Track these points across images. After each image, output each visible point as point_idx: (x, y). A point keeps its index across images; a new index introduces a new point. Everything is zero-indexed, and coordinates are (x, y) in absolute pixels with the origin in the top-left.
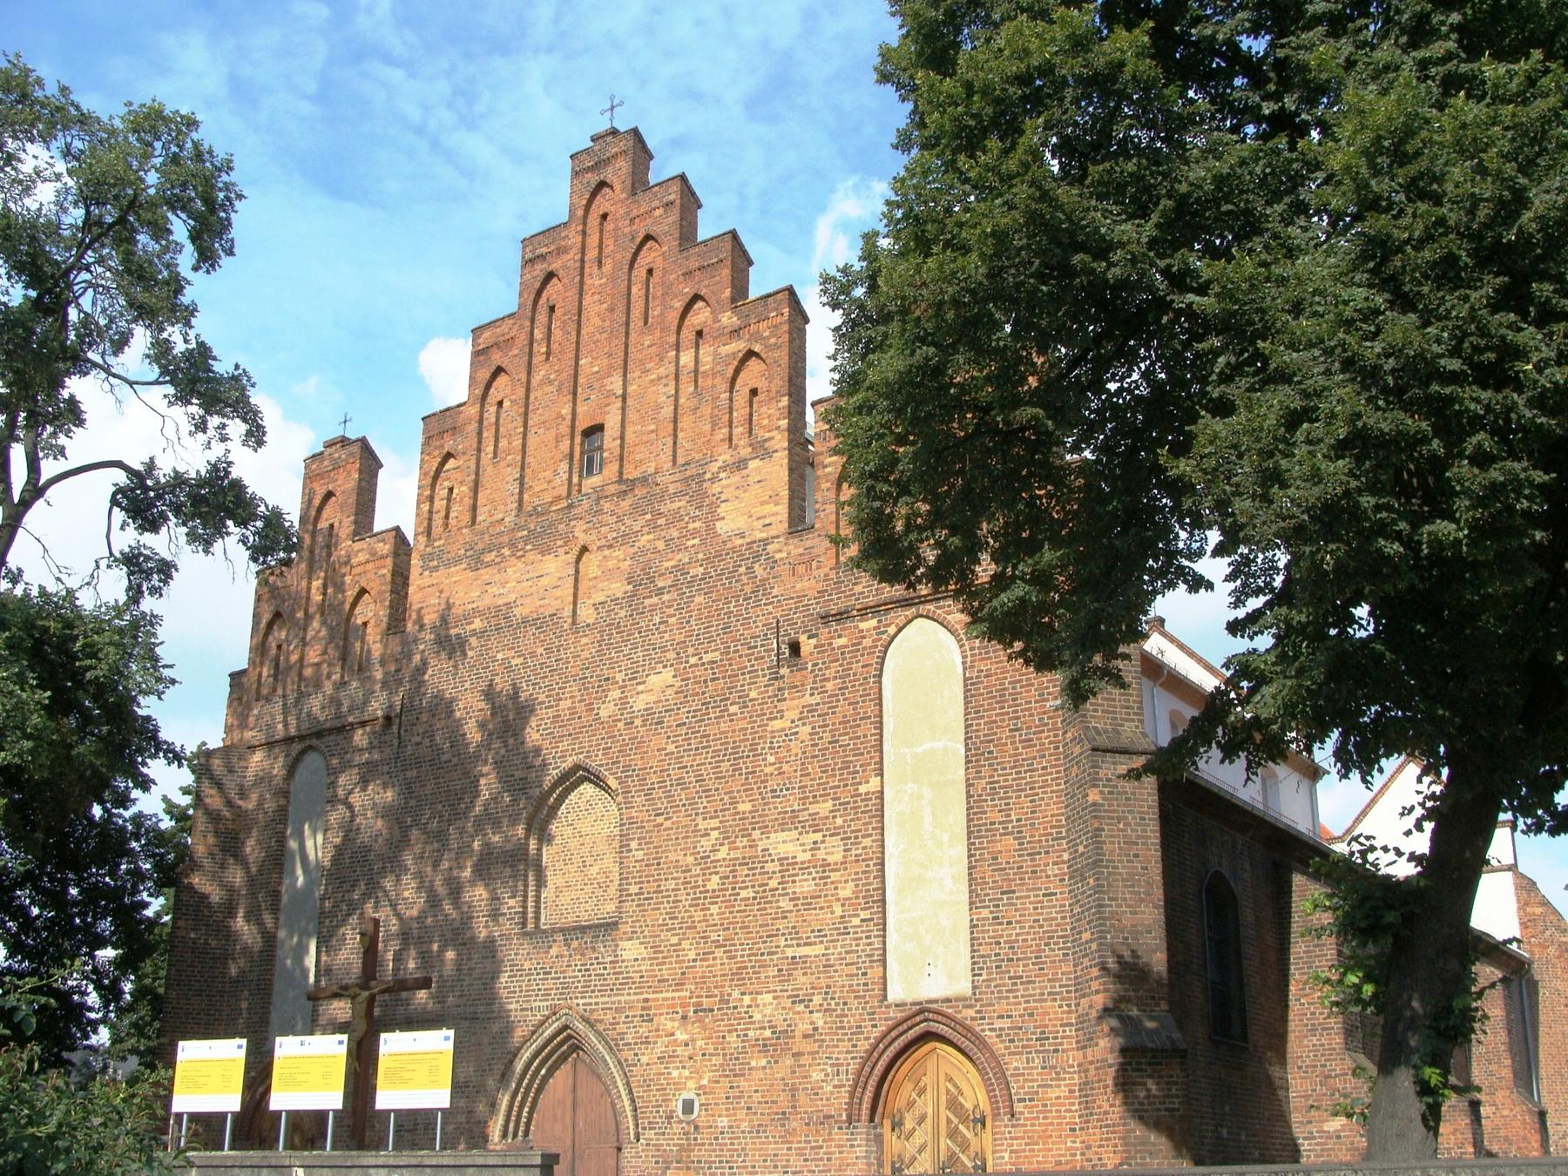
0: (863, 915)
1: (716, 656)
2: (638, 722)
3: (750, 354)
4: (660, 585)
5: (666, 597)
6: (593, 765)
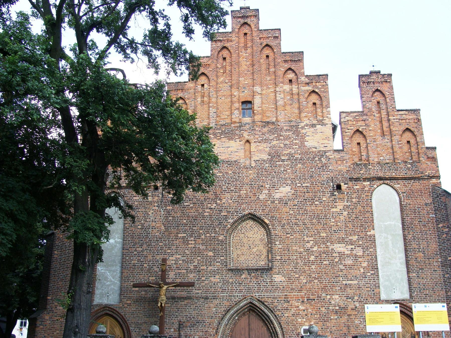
0: (372, 272)
2: (277, 202)
3: (314, 92)
4: (283, 158)
5: (286, 163)
6: (258, 214)
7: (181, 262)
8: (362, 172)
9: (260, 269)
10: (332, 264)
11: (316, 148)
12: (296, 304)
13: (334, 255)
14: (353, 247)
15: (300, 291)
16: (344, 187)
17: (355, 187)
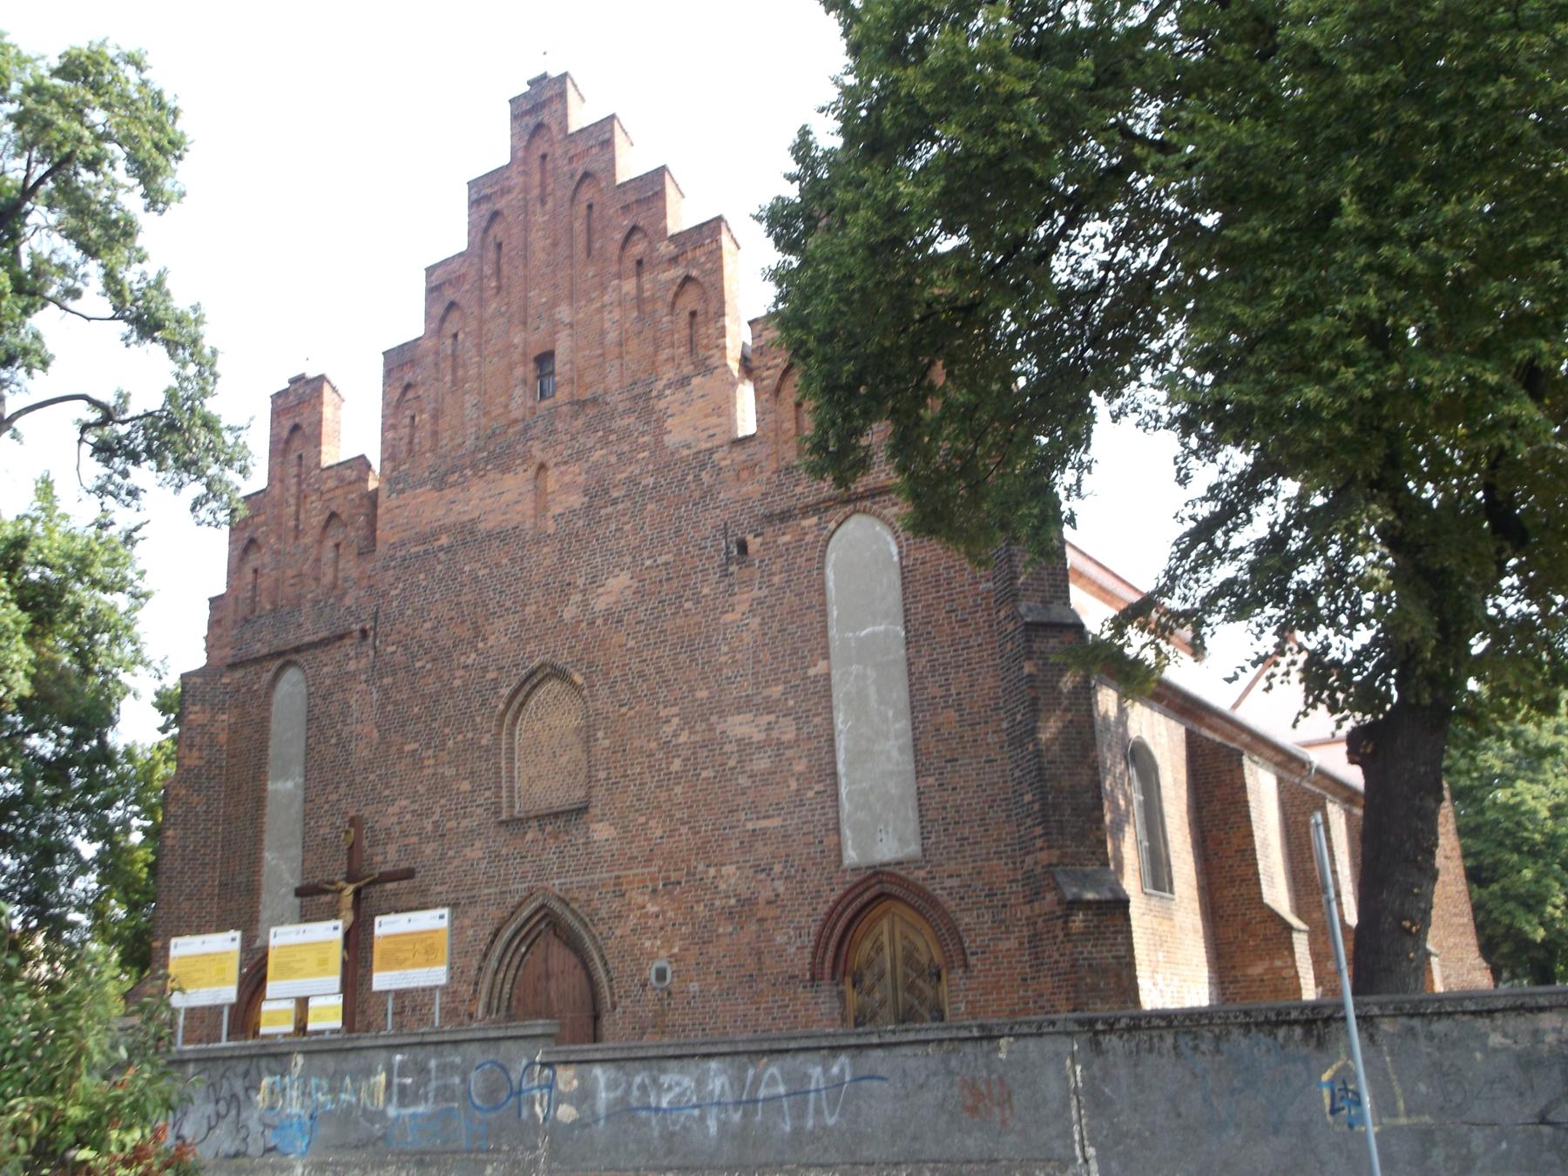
1: (669, 557)
2: (599, 622)
4: (615, 495)
5: (620, 507)
9: (563, 812)
11: (688, 447)
12: (640, 900)
13: (727, 748)
14: (772, 718)
15: (648, 861)
16: (754, 544)
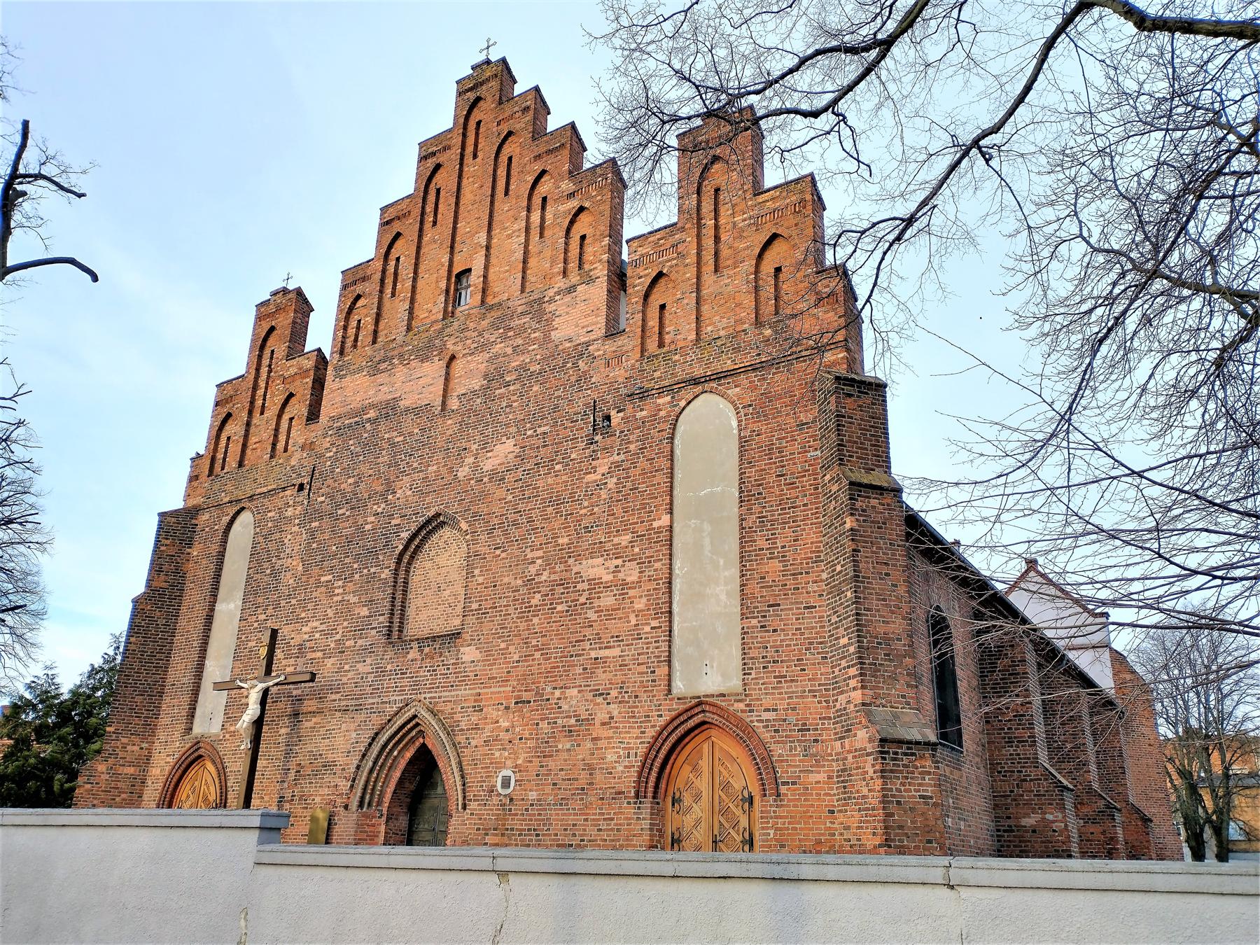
2: (485, 479)
5: (512, 388)
7: (317, 636)
8: (657, 374)
10: (574, 610)
11: (570, 340)
13: (579, 587)
14: (619, 562)
16: (616, 418)
17: (639, 415)
